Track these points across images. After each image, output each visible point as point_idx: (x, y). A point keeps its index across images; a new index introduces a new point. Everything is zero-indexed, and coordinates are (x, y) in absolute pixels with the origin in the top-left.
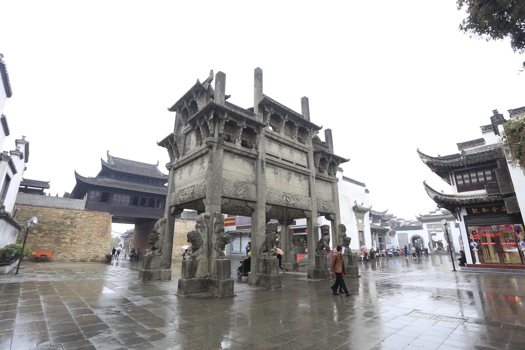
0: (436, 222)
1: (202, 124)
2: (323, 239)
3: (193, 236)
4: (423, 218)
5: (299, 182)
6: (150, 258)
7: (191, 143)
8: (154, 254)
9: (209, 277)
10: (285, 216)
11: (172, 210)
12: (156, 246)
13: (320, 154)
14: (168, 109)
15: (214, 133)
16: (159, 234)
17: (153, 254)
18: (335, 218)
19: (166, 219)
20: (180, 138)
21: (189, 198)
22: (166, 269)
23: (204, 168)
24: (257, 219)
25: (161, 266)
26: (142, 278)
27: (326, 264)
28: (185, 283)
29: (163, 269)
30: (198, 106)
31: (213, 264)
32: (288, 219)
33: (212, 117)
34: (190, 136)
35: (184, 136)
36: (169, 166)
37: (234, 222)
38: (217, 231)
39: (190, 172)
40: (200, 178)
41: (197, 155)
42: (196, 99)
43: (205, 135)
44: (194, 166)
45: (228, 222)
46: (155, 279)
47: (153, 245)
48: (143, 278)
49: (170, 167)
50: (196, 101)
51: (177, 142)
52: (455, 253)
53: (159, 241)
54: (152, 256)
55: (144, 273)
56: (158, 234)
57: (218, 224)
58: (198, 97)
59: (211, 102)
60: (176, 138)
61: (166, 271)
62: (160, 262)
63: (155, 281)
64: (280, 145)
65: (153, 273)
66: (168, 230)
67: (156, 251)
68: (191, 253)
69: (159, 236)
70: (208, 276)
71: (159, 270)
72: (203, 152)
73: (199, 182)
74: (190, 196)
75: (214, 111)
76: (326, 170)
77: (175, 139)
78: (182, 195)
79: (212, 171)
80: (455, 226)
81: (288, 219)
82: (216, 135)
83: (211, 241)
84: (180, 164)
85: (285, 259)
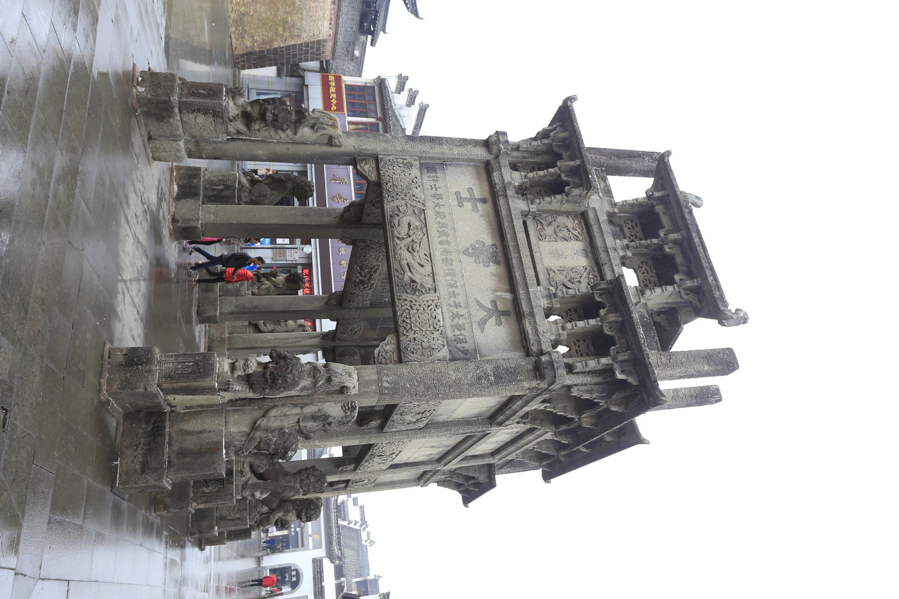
0: (325, 523)
1: (607, 331)
2: (288, 512)
3: (289, 381)
4: (333, 499)
5: (427, 454)
6: (217, 114)
7: (561, 245)
8: (231, 121)
9: (173, 411)
10: (345, 344)
11: (366, 168)
12: (256, 126)
13: (487, 480)
14: (669, 153)
15: (573, 374)
16: (295, 133)
17: (229, 119)
18: (337, 489)
19: (340, 146)
20: (575, 202)
21: (399, 269)
22: (186, 150)
23: (483, 323)
24: (337, 436)
25: (194, 137)
26: (149, 96)
27: (229, 520)
28: (146, 389)
29: (186, 142)
30: (658, 290)
31: (209, 423)
32: (338, 351)
33: (620, 376)
34: (577, 239)
35: (582, 209)
36: (500, 150)
37: (334, 108)
38: (305, 427)
39: (473, 251)
40: (455, 310)
41: (521, 292)
42: (679, 287)
43: (573, 331)
44: (493, 268)
45: (333, 89)
46: (151, 127)
47: (257, 119)
48: (150, 101)
49: (495, 151)
50: (671, 282)
51: (567, 196)
52: (262, 556)
53: (272, 133)
54: (222, 118)
55: (165, 100)
56: (293, 130)
57: (324, 426)
58: (683, 294)
59: (662, 402)
60: (580, 196)
61: (178, 150)
62: (205, 135)
63: (143, 128)
64: (517, 432)
65: (169, 122)
66: (308, 153)
67: (240, 125)
68: (239, 372)
69: (289, 132)
70: (173, 409)
71: (179, 136)
72: (527, 324)
73: (447, 315)
74: (406, 277)
75: (636, 386)
76: (448, 477)
77: (576, 191)
78: (409, 225)
79: (470, 385)
80: (315, 558)
81: (337, 353)
82: (569, 380)
83: (274, 407)
84: (502, 201)
85: (237, 346)
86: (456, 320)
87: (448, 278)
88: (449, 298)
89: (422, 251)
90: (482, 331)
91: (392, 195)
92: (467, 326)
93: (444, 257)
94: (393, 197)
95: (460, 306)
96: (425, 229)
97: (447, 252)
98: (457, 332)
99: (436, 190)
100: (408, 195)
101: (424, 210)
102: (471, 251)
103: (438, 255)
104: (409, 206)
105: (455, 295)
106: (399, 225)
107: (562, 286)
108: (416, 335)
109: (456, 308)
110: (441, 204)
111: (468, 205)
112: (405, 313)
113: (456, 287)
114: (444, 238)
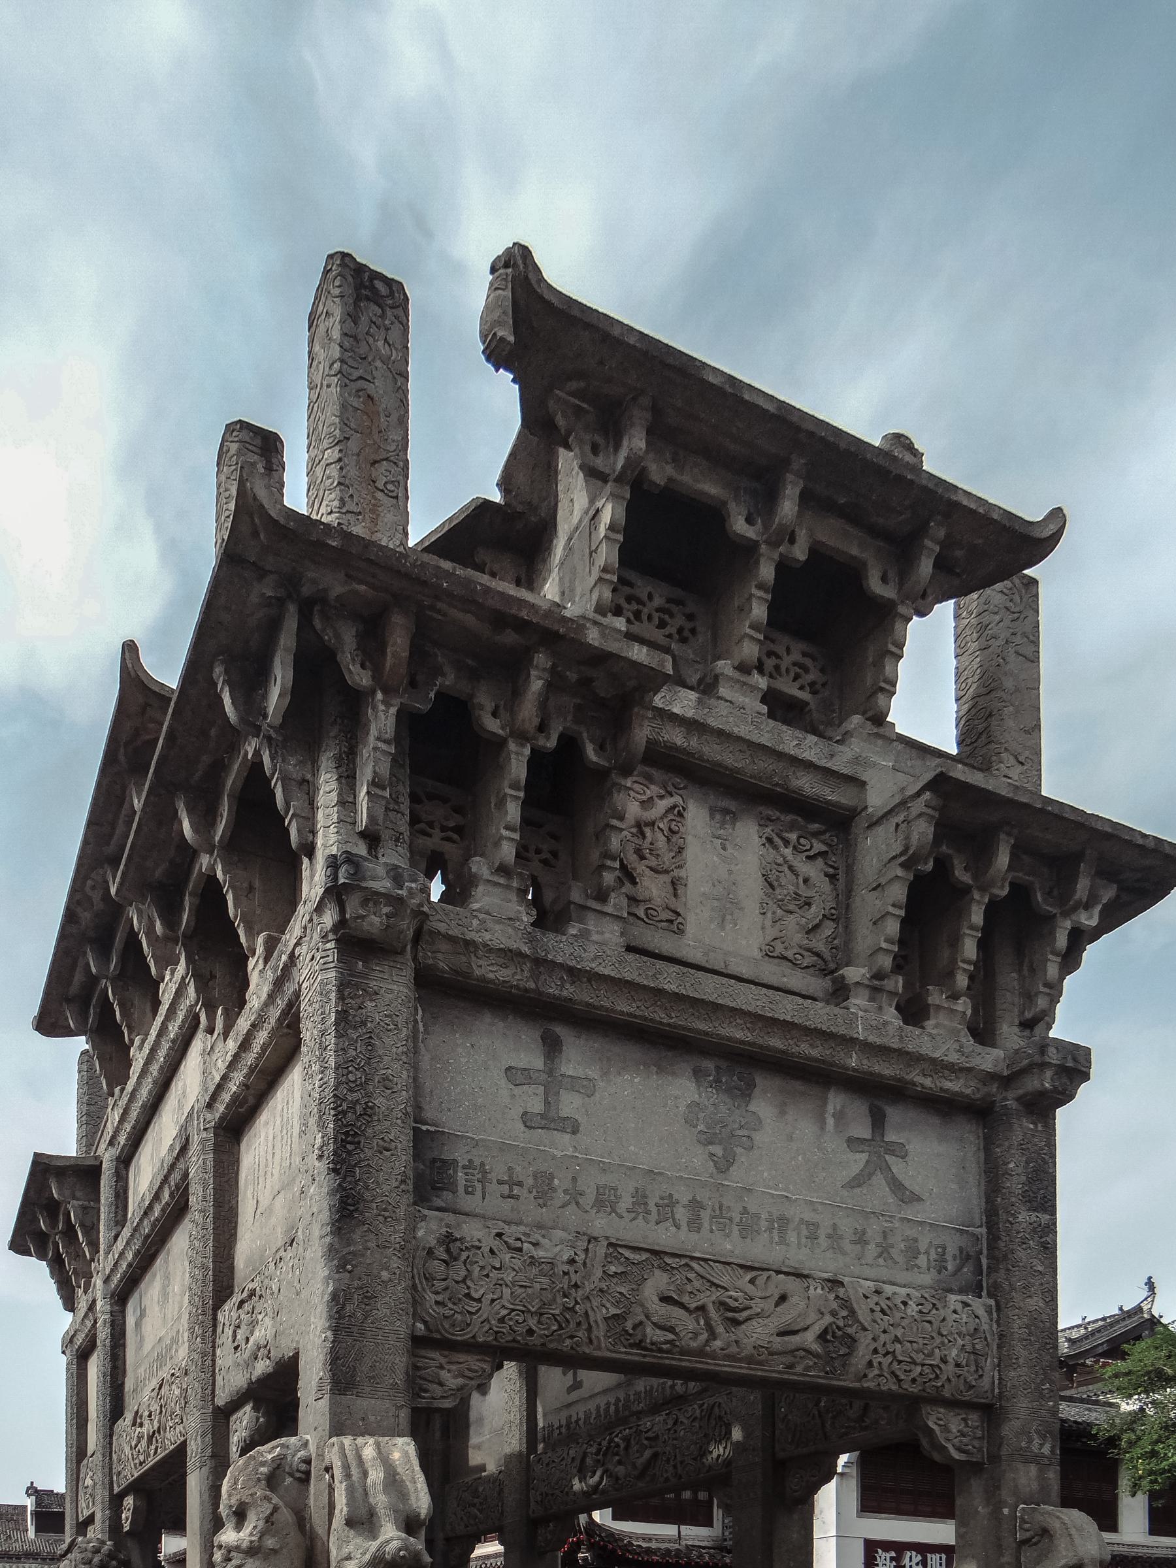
72: (928, 1082)
73: (902, 1277)
86: (894, 1252)
87: (792, 1237)
88: (845, 1254)
89: (738, 1286)
90: (919, 1199)
91: (572, 1325)
92: (911, 1232)
93: (735, 1229)
94: (579, 1324)
95: (864, 1232)
96: (668, 1260)
97: (721, 1215)
98: (922, 1261)
99: (520, 1184)
100: (575, 1278)
101: (610, 1244)
102: (718, 1150)
103: (760, 1250)
104: (603, 1285)
105: (835, 1236)
106: (671, 1330)
107: (811, 936)
108: (950, 1359)
109: (867, 1243)
110: (567, 1184)
111: (570, 1104)
112: (898, 1373)
113: (816, 1225)
114: (681, 1214)
